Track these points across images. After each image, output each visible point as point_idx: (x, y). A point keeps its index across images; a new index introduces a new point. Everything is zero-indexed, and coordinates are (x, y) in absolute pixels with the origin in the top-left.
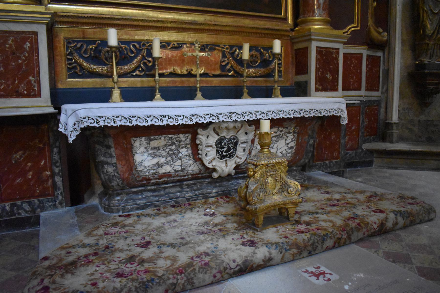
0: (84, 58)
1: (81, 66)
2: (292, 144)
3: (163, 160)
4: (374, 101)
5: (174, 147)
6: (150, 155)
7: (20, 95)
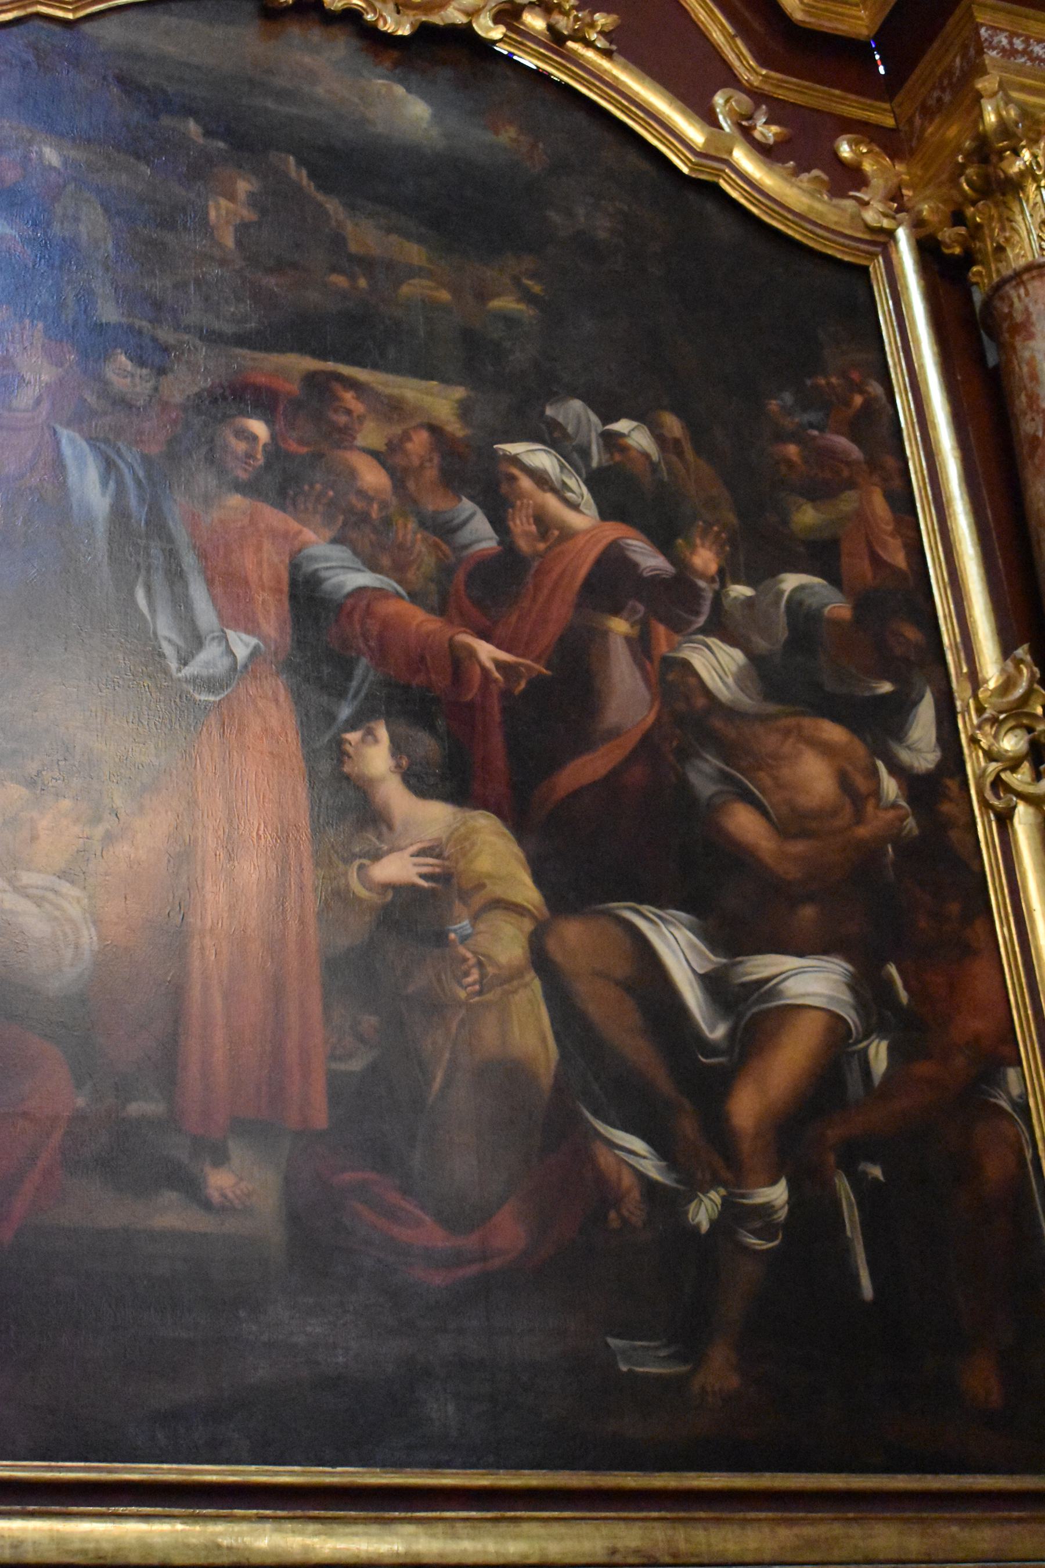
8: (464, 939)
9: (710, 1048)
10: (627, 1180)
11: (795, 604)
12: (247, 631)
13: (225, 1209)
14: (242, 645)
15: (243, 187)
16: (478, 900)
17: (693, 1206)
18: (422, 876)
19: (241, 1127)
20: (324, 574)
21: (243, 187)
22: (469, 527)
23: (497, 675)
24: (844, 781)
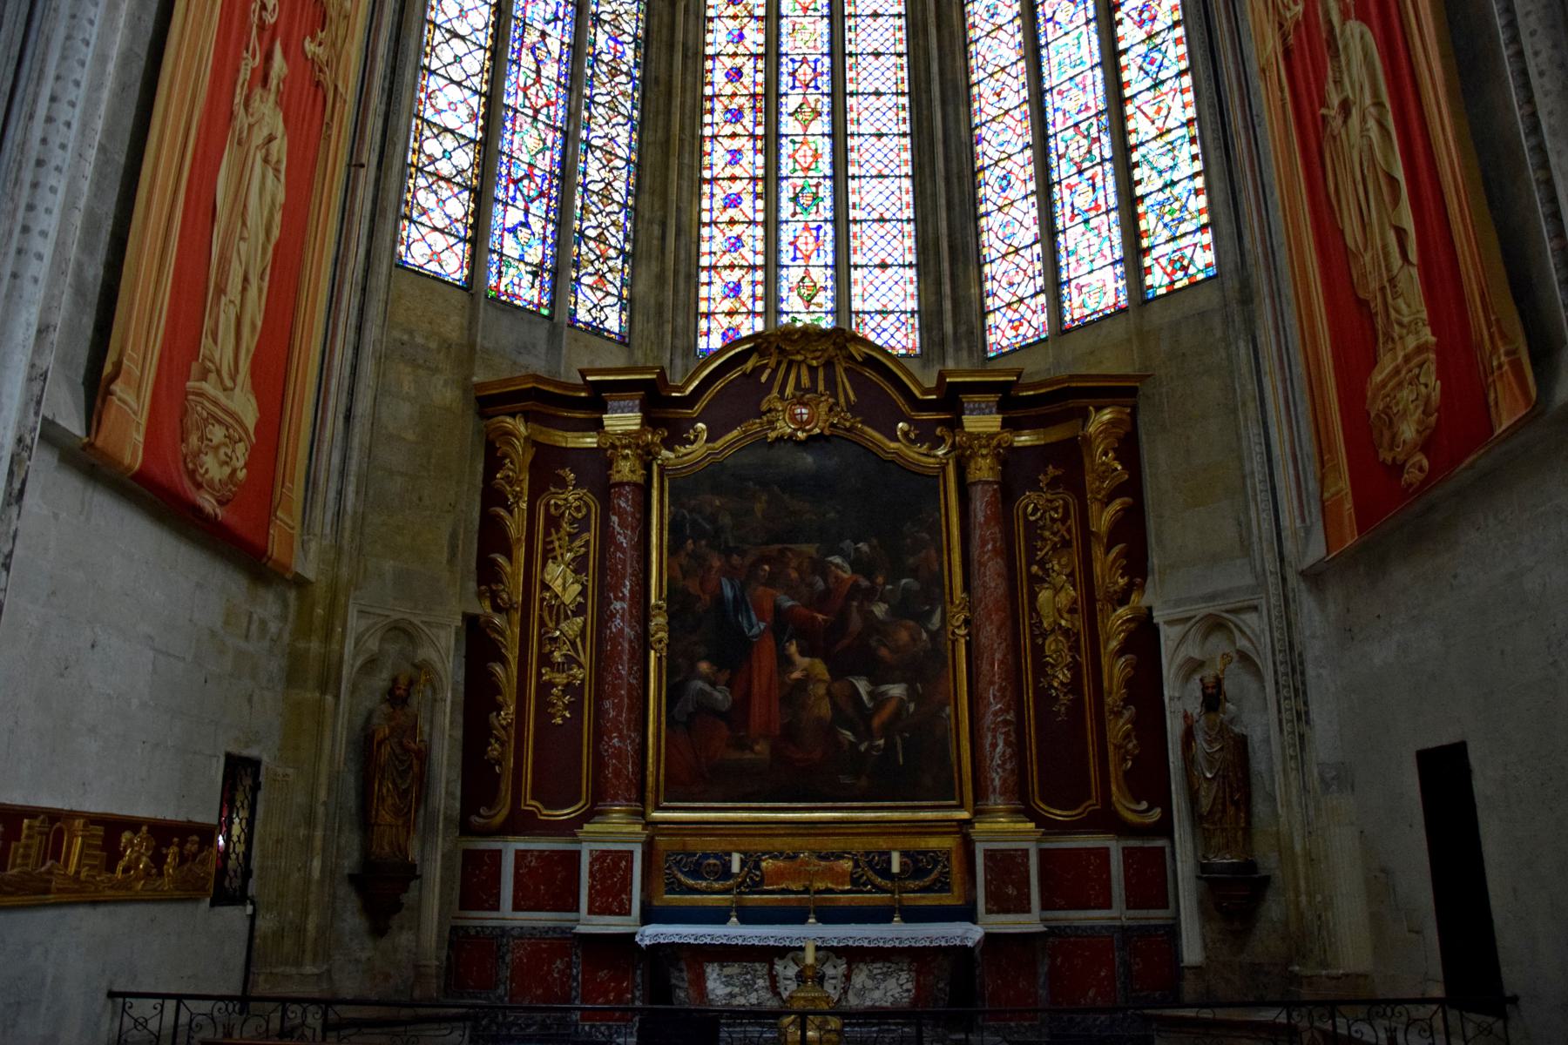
0: (683, 872)
1: (679, 881)
2: (909, 986)
3: (737, 990)
4: (1156, 927)
5: (748, 977)
6: (722, 983)
7: (612, 913)
9: (869, 709)
11: (906, 589)
15: (764, 498)
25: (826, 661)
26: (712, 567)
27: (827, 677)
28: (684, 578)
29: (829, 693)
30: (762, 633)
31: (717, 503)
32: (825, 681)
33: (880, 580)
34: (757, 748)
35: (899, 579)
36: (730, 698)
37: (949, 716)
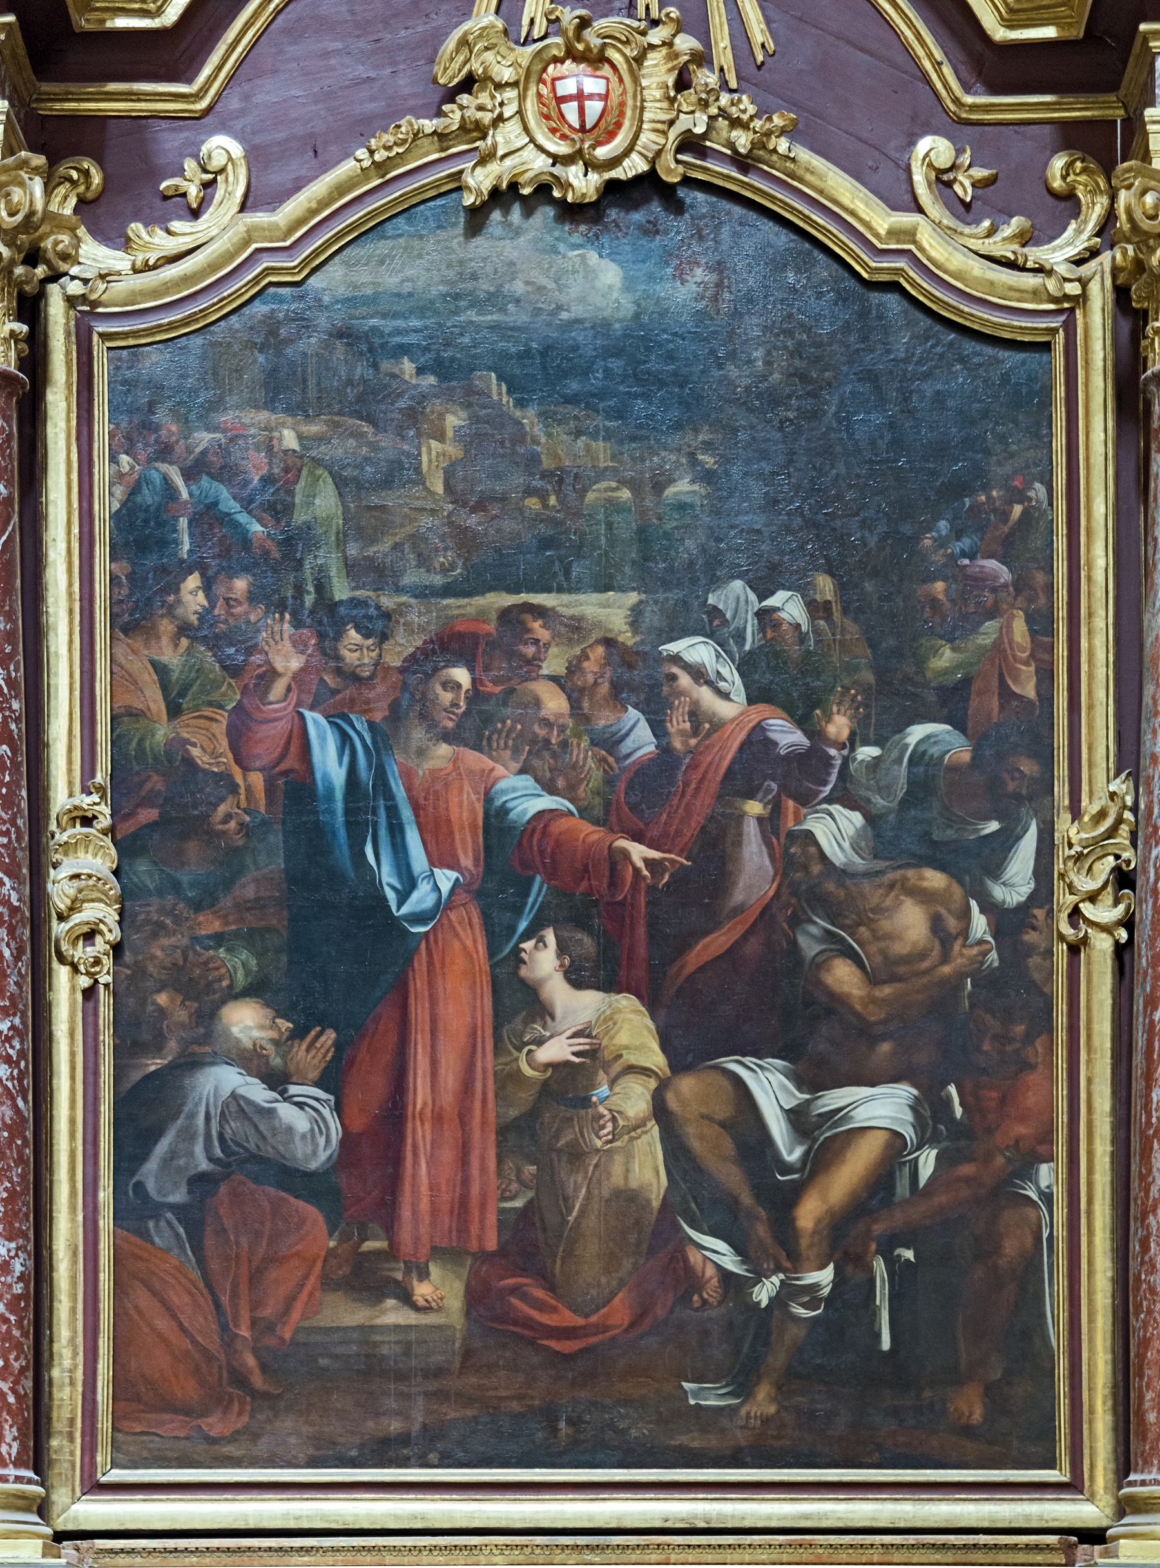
8: (602, 1101)
9: (786, 1169)
10: (710, 1271)
11: (918, 757)
12: (451, 868)
13: (426, 1309)
14: (446, 879)
15: (454, 421)
16: (617, 1068)
17: (756, 1289)
18: (574, 1054)
19: (437, 1252)
20: (510, 805)
21: (454, 421)
22: (632, 736)
23: (646, 873)
24: (936, 925)
25: (652, 1004)
26: (271, 674)
27: (656, 1059)
28: (174, 710)
29: (660, 1110)
30: (443, 907)
31: (289, 439)
32: (646, 1071)
33: (839, 726)
34: (422, 1291)
35: (901, 727)
36: (335, 1127)
37: (1047, 1197)
